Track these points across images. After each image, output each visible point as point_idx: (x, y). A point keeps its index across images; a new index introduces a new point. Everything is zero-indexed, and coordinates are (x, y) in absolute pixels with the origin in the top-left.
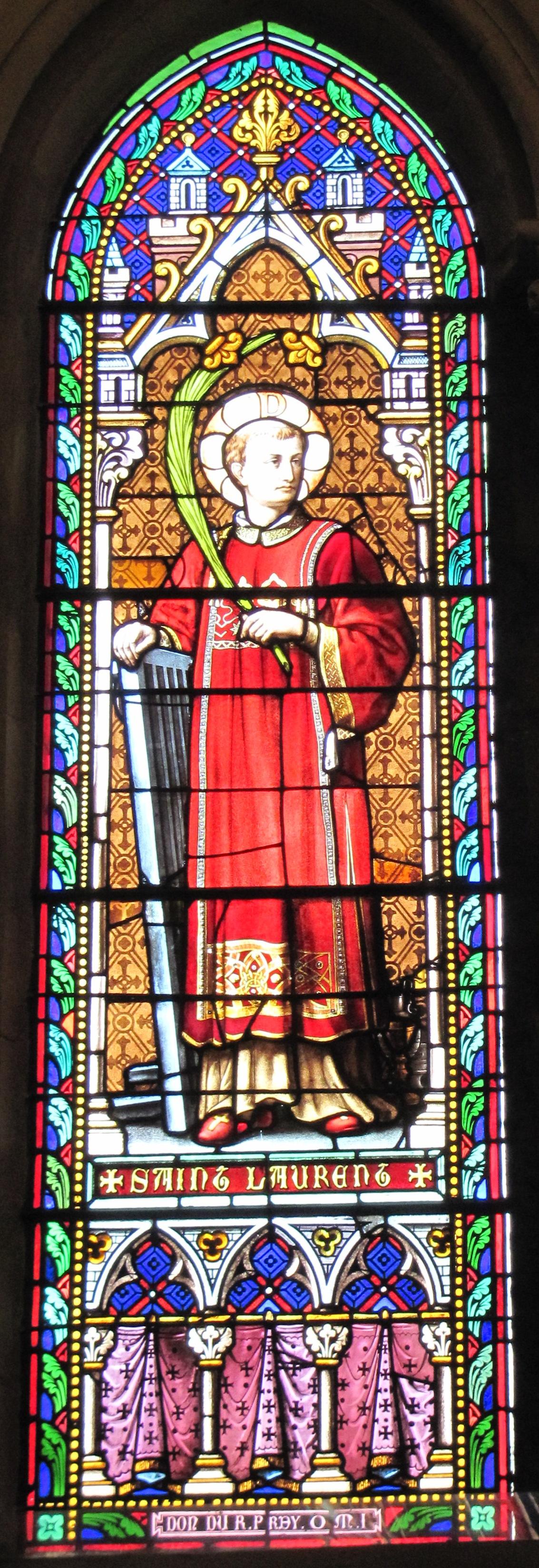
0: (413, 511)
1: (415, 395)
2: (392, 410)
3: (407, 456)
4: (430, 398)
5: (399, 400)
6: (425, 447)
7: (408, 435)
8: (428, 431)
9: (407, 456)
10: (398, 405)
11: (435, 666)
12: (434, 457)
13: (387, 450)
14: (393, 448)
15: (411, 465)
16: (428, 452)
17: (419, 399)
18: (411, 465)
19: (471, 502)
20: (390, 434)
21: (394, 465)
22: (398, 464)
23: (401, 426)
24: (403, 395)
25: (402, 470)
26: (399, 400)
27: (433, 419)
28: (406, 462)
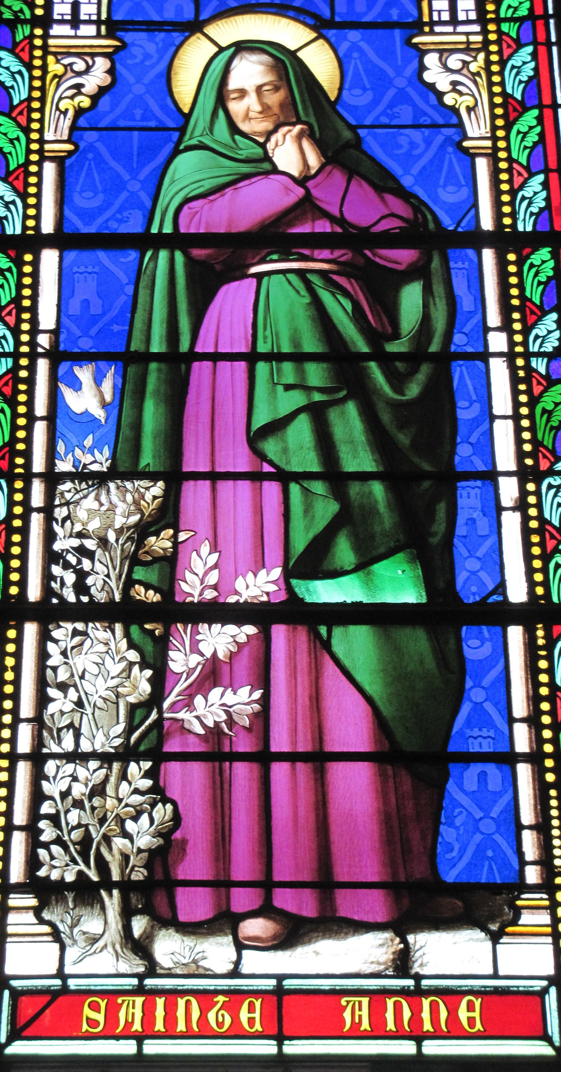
0: (466, 144)
1: (461, 16)
2: (432, 33)
3: (454, 84)
4: (482, 19)
5: (441, 23)
6: (478, 74)
7: (454, 61)
8: (481, 56)
9: (454, 84)
10: (437, 29)
11: (506, 327)
12: (491, 84)
13: (428, 77)
14: (435, 74)
15: (461, 94)
16: (483, 82)
17: (468, 22)
18: (461, 94)
19: (542, 135)
20: (431, 60)
21: (440, 95)
22: (443, 94)
23: (444, 52)
24: (446, 16)
25: (449, 100)
26: (441, 23)
27: (486, 43)
28: (454, 90)
